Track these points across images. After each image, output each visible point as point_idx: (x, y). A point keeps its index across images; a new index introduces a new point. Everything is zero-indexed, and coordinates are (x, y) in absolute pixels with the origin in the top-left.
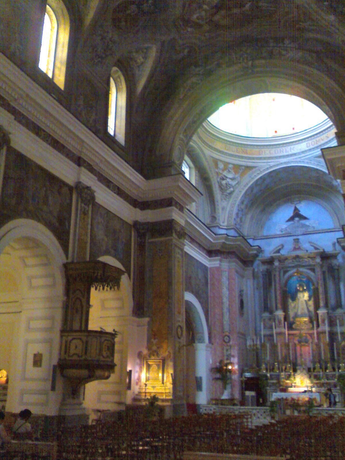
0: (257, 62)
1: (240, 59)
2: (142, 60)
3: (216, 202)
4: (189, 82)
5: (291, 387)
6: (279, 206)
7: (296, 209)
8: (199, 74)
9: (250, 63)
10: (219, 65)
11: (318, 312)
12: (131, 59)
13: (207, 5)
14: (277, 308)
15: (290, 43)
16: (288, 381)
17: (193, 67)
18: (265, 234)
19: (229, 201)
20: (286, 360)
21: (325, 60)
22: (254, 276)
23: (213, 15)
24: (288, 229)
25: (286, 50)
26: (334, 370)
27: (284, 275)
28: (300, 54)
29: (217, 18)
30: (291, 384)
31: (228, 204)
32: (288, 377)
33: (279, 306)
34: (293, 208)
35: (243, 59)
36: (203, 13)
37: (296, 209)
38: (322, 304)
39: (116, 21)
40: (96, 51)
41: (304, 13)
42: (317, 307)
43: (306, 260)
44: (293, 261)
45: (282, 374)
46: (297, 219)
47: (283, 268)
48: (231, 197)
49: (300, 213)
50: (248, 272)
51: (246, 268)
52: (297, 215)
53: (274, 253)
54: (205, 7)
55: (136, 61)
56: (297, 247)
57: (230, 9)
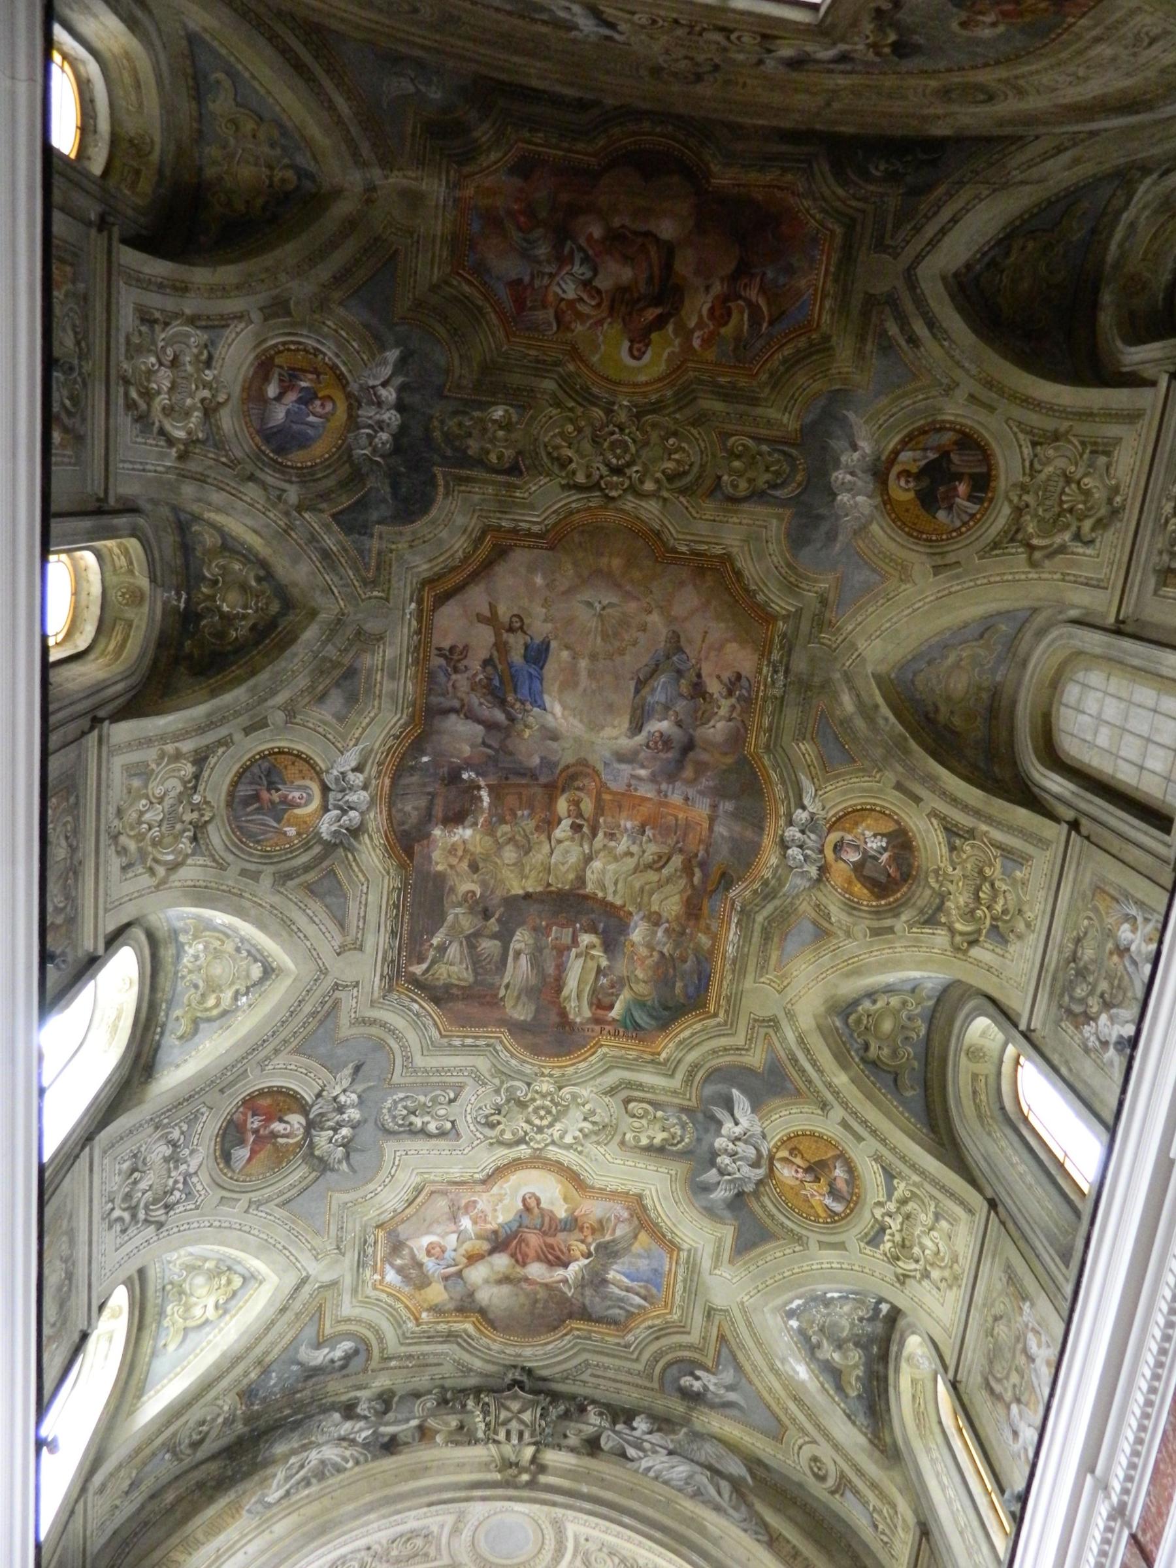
0: (551, 1457)
1: (496, 1432)
2: (211, 1313)
4: (314, 1456)
8: (353, 1442)
9: (529, 1451)
10: (424, 1433)
12: (181, 1293)
13: (475, 1223)
15: (650, 1433)
17: (337, 1416)
21: (759, 1507)
23: (473, 1258)
25: (639, 1447)
28: (681, 1470)
29: (477, 1274)
35: (508, 1433)
36: (452, 1241)
39: (231, 1135)
40: (135, 1182)
41: (722, 1338)
54: (466, 1223)
55: (188, 1308)
57: (521, 1260)
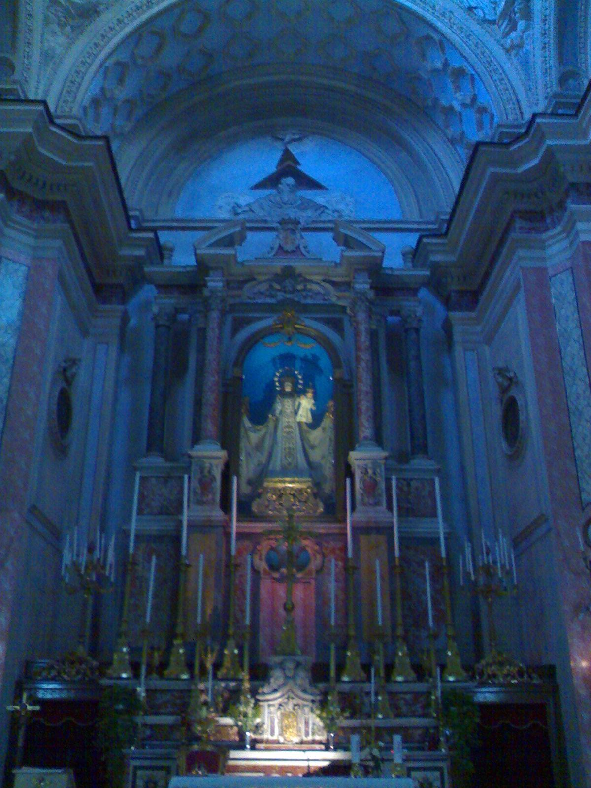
3: (22, 16)
5: (241, 747)
6: (232, 142)
7: (287, 155)
11: (353, 455)
14: (196, 439)
16: (228, 721)
18: (179, 214)
19: (72, 41)
20: (220, 628)
22: (125, 339)
24: (255, 208)
26: (420, 672)
27: (235, 331)
30: (241, 735)
31: (67, 48)
32: (229, 703)
33: (210, 426)
34: (277, 155)
37: (287, 155)
38: (365, 430)
42: (345, 438)
43: (315, 287)
44: (271, 286)
45: (201, 686)
46: (290, 181)
47: (233, 308)
48: (78, 30)
49: (300, 168)
50: (109, 318)
51: (101, 307)
52: (289, 168)
53: (212, 245)
56: (289, 247)
